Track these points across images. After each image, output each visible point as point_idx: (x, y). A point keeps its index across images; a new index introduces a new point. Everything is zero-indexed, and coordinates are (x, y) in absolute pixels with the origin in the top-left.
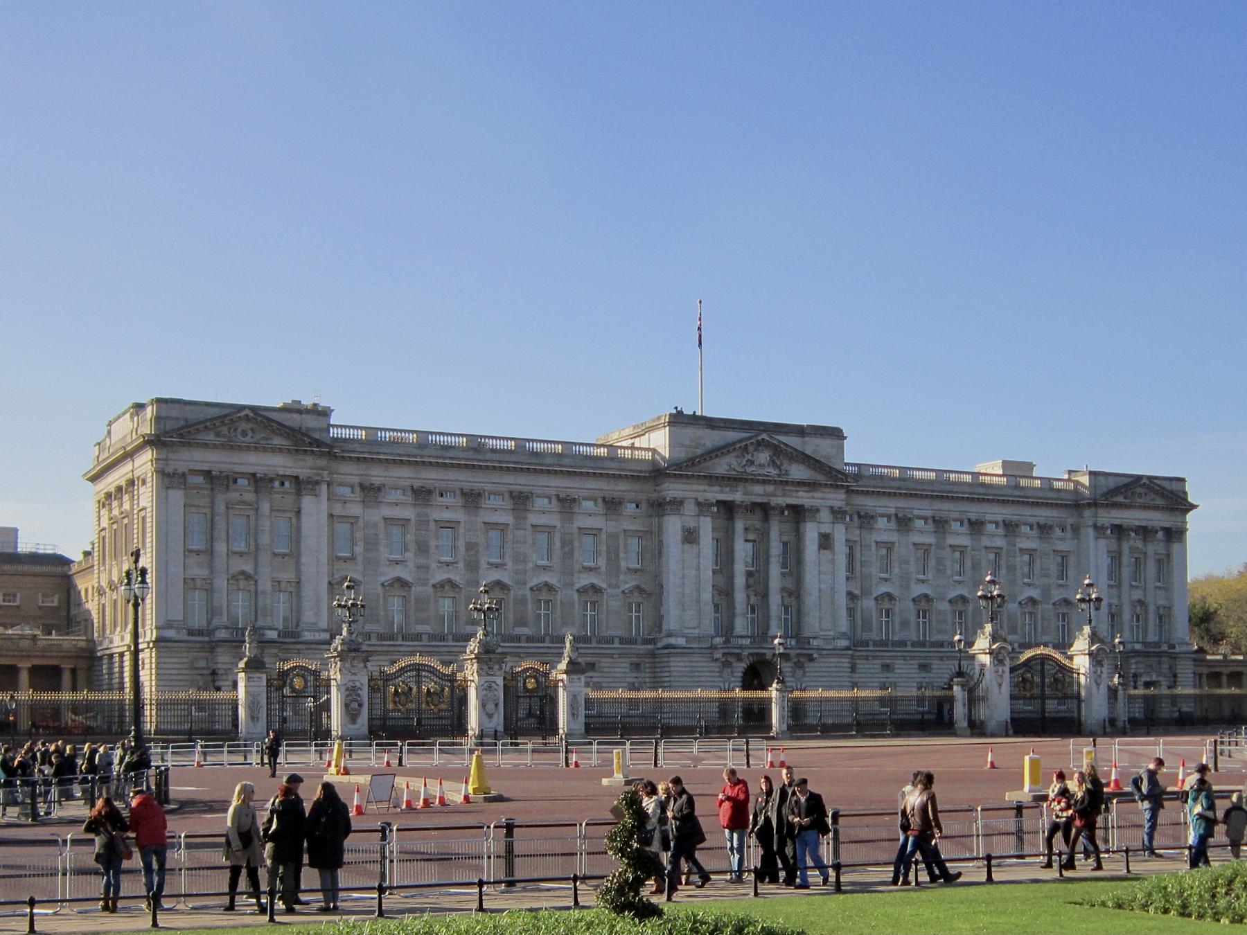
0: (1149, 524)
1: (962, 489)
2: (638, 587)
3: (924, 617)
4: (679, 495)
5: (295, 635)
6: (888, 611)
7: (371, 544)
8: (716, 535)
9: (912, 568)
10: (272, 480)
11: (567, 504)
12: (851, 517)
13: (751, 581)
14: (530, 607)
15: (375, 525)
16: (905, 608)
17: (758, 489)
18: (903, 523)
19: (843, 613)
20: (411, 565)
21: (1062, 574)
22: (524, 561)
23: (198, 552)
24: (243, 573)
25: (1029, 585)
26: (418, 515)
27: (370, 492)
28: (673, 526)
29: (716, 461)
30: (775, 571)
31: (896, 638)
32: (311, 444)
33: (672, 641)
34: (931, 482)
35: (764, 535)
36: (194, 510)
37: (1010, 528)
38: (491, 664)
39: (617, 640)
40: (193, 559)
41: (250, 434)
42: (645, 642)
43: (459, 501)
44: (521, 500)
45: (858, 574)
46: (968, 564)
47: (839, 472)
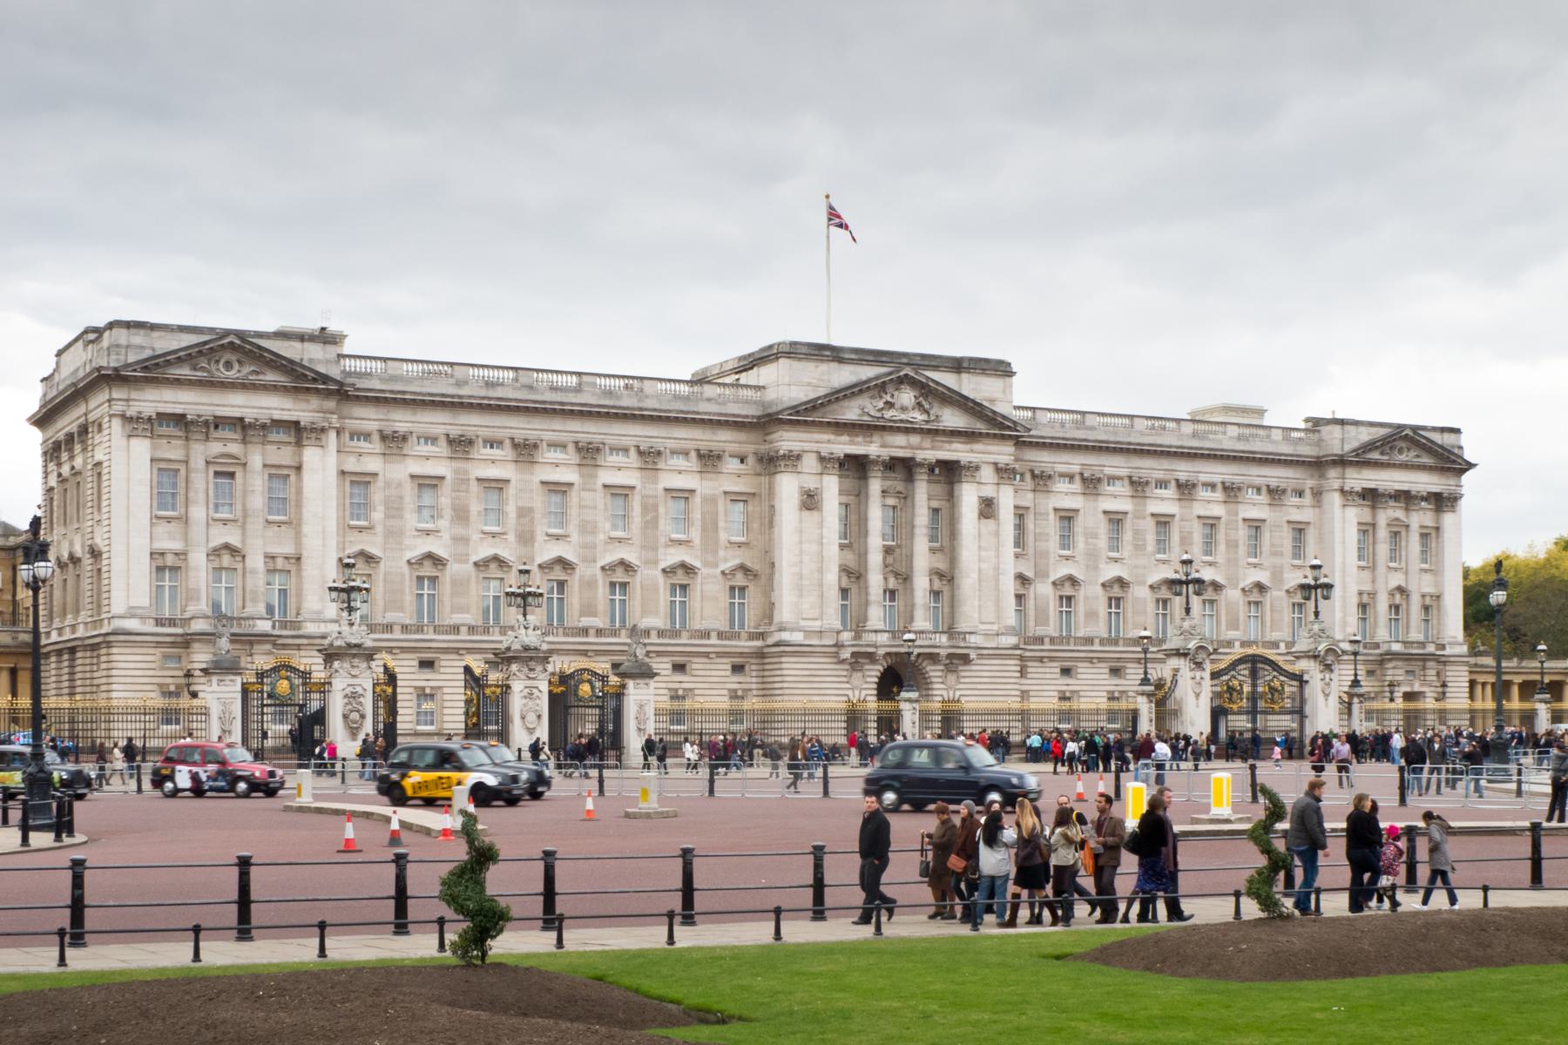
0: (1414, 488)
2: (743, 568)
3: (1118, 607)
4: (796, 446)
5: (296, 625)
7: (394, 510)
8: (845, 499)
9: (1103, 542)
10: (264, 426)
11: (650, 457)
12: (1022, 475)
13: (890, 560)
14: (600, 590)
15: (400, 485)
17: (900, 439)
18: (1091, 484)
19: (1012, 600)
20: (446, 536)
21: (1298, 550)
22: (594, 532)
23: (169, 520)
24: (227, 547)
26: (456, 472)
27: (394, 441)
28: (788, 486)
29: (845, 403)
30: (921, 545)
31: (1080, 634)
32: (314, 380)
33: (786, 636)
35: (906, 497)
36: (163, 465)
37: (1231, 491)
38: (532, 664)
39: (713, 634)
40: (162, 528)
41: (236, 366)
42: (752, 636)
43: (507, 452)
44: (589, 453)
45: (1031, 551)
46: (1175, 538)
47: (1004, 417)
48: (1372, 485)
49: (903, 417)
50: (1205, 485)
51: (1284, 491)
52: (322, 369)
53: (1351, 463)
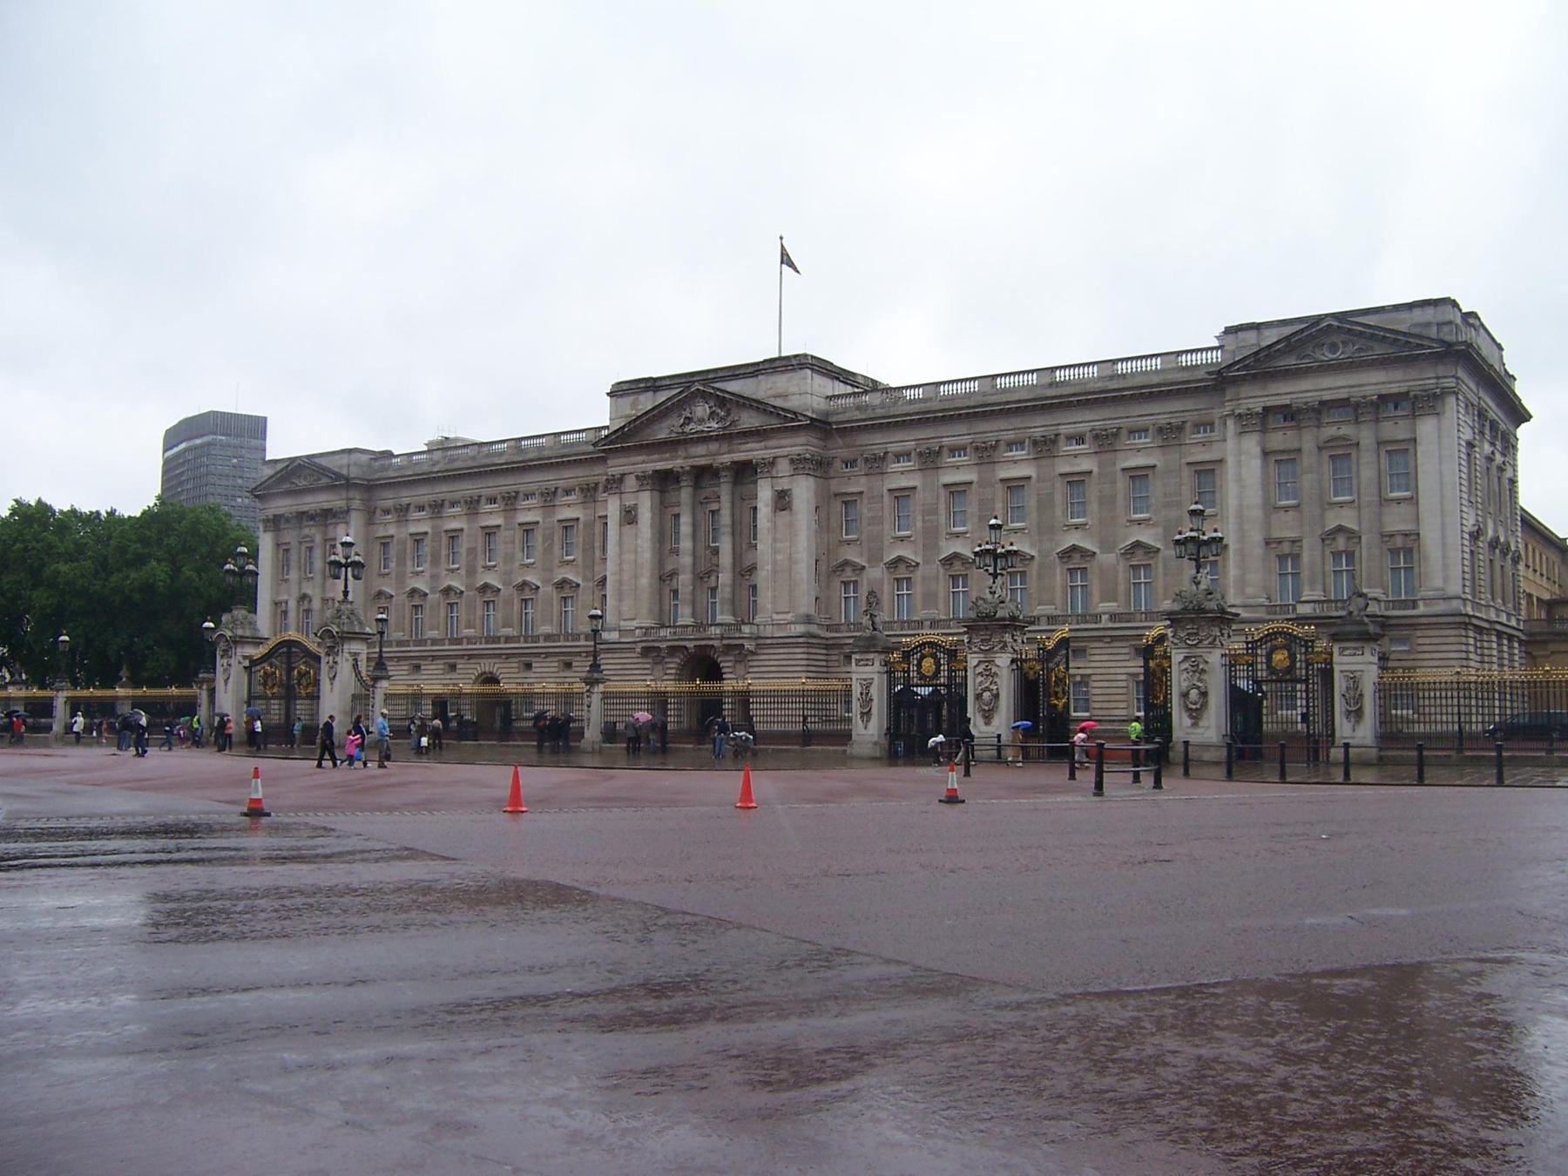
0: (1356, 393)
1: (1016, 397)
6: (908, 579)
7: (401, 561)
9: (942, 519)
15: (404, 542)
16: (930, 576)
17: (701, 449)
18: (930, 459)
20: (427, 574)
25: (1139, 522)
29: (657, 427)
34: (970, 395)
37: (1105, 441)
45: (864, 537)
46: (1031, 502)
48: (1286, 400)
49: (700, 428)
50: (1069, 438)
51: (1180, 428)
52: (344, 472)
53: (1244, 379)
